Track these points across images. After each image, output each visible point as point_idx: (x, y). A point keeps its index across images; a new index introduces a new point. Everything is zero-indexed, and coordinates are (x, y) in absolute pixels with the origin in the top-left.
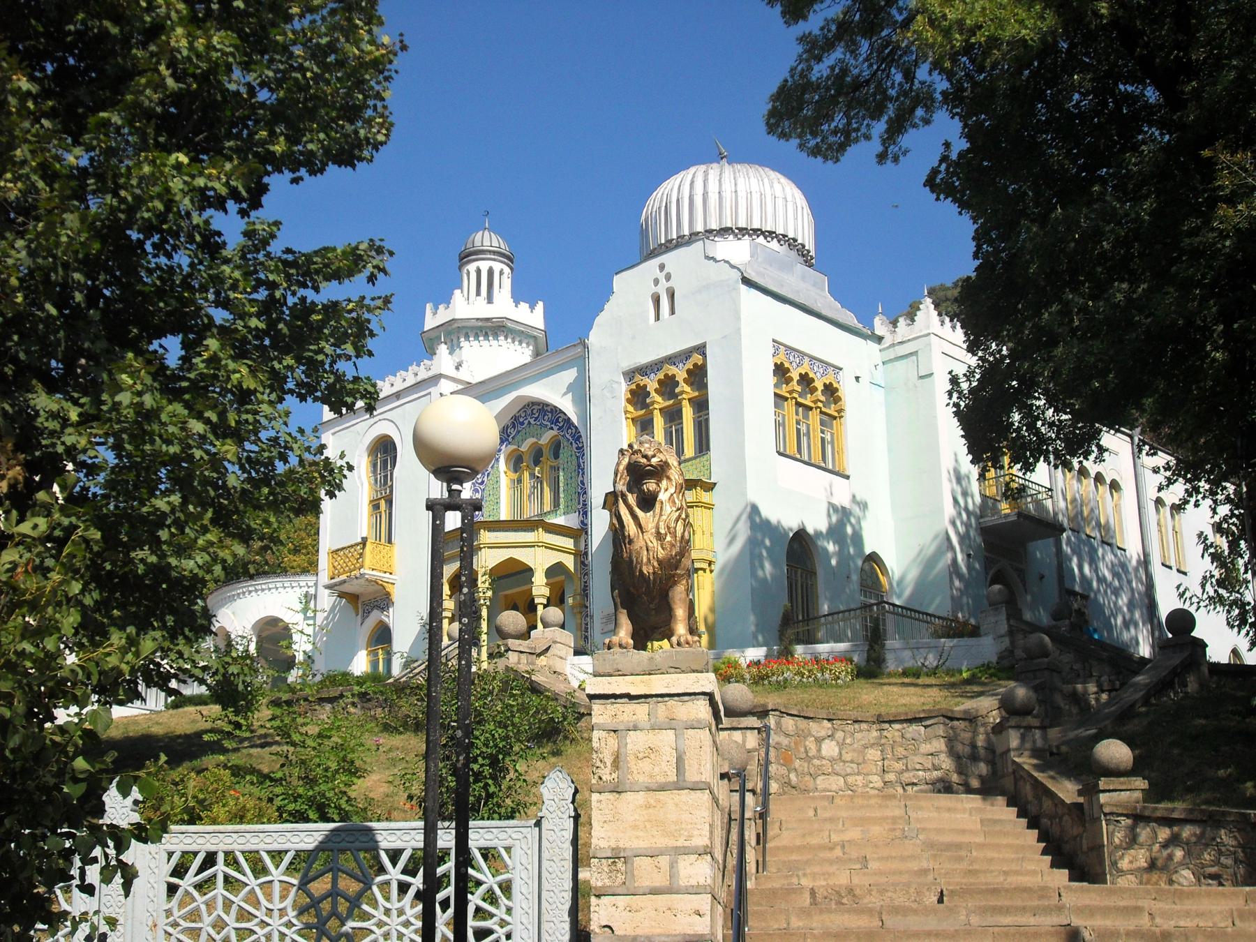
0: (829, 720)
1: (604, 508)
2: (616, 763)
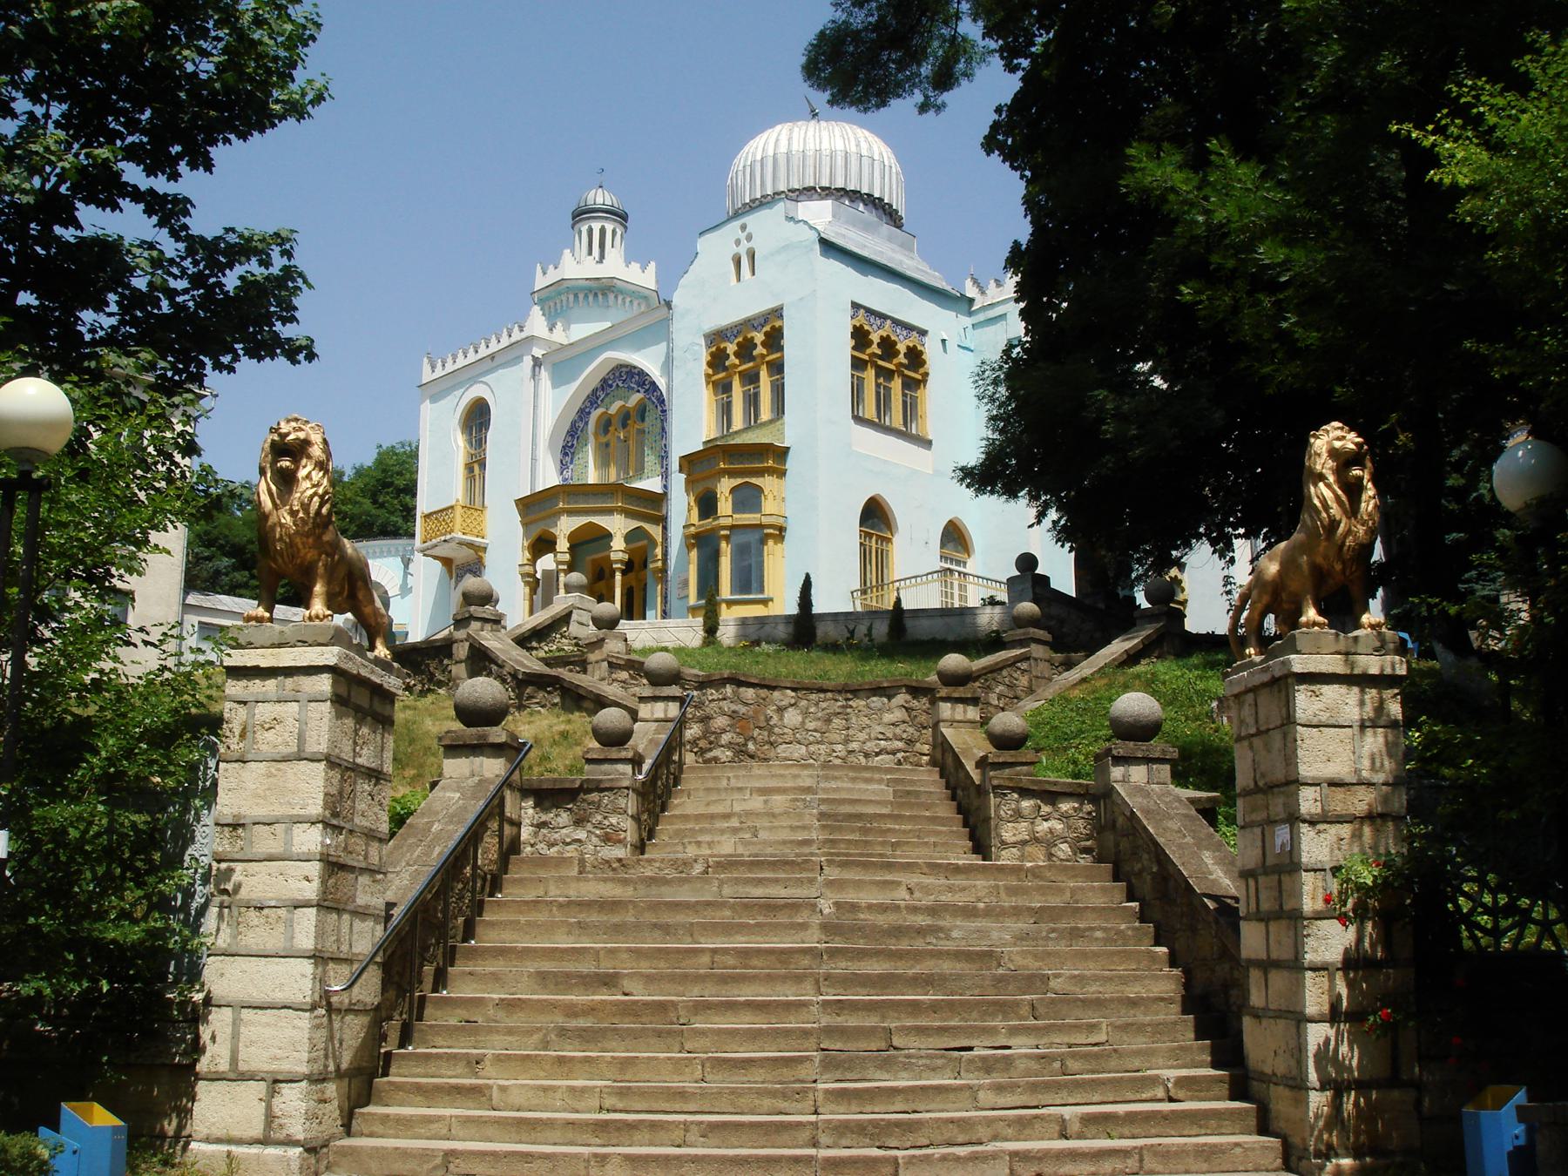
0: (793, 689)
1: (681, 471)
2: (243, 735)
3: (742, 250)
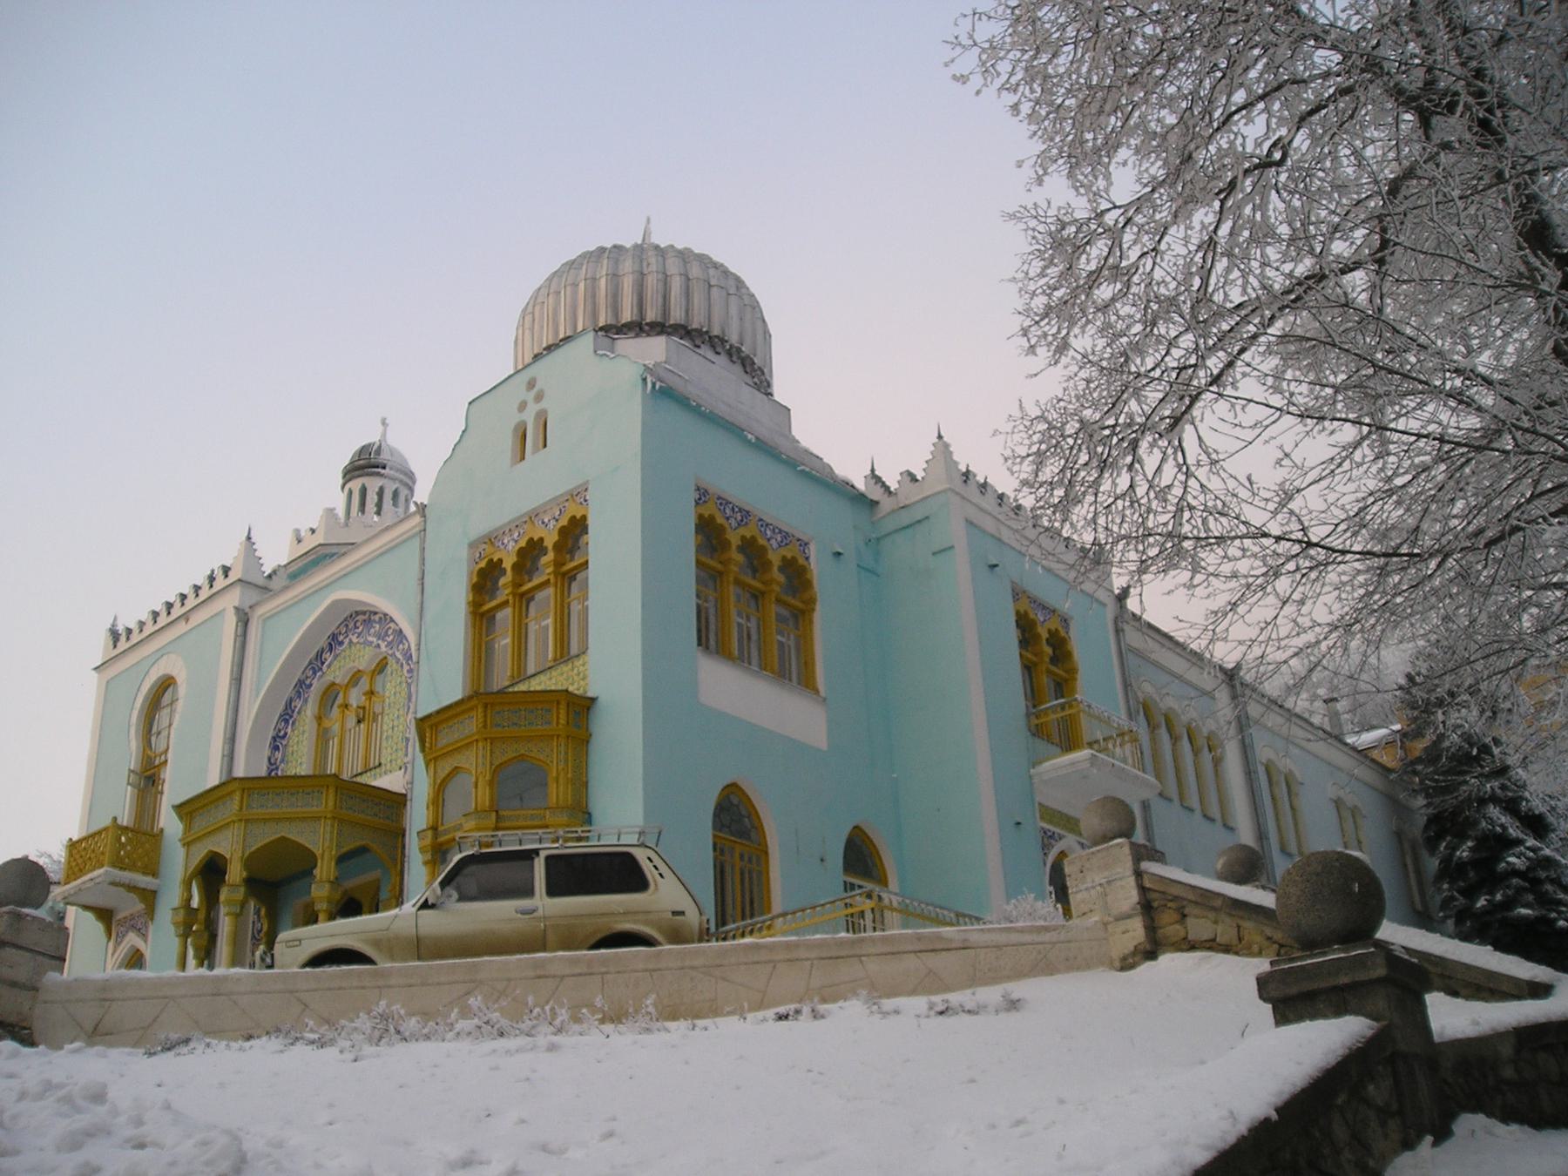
3: (529, 416)
